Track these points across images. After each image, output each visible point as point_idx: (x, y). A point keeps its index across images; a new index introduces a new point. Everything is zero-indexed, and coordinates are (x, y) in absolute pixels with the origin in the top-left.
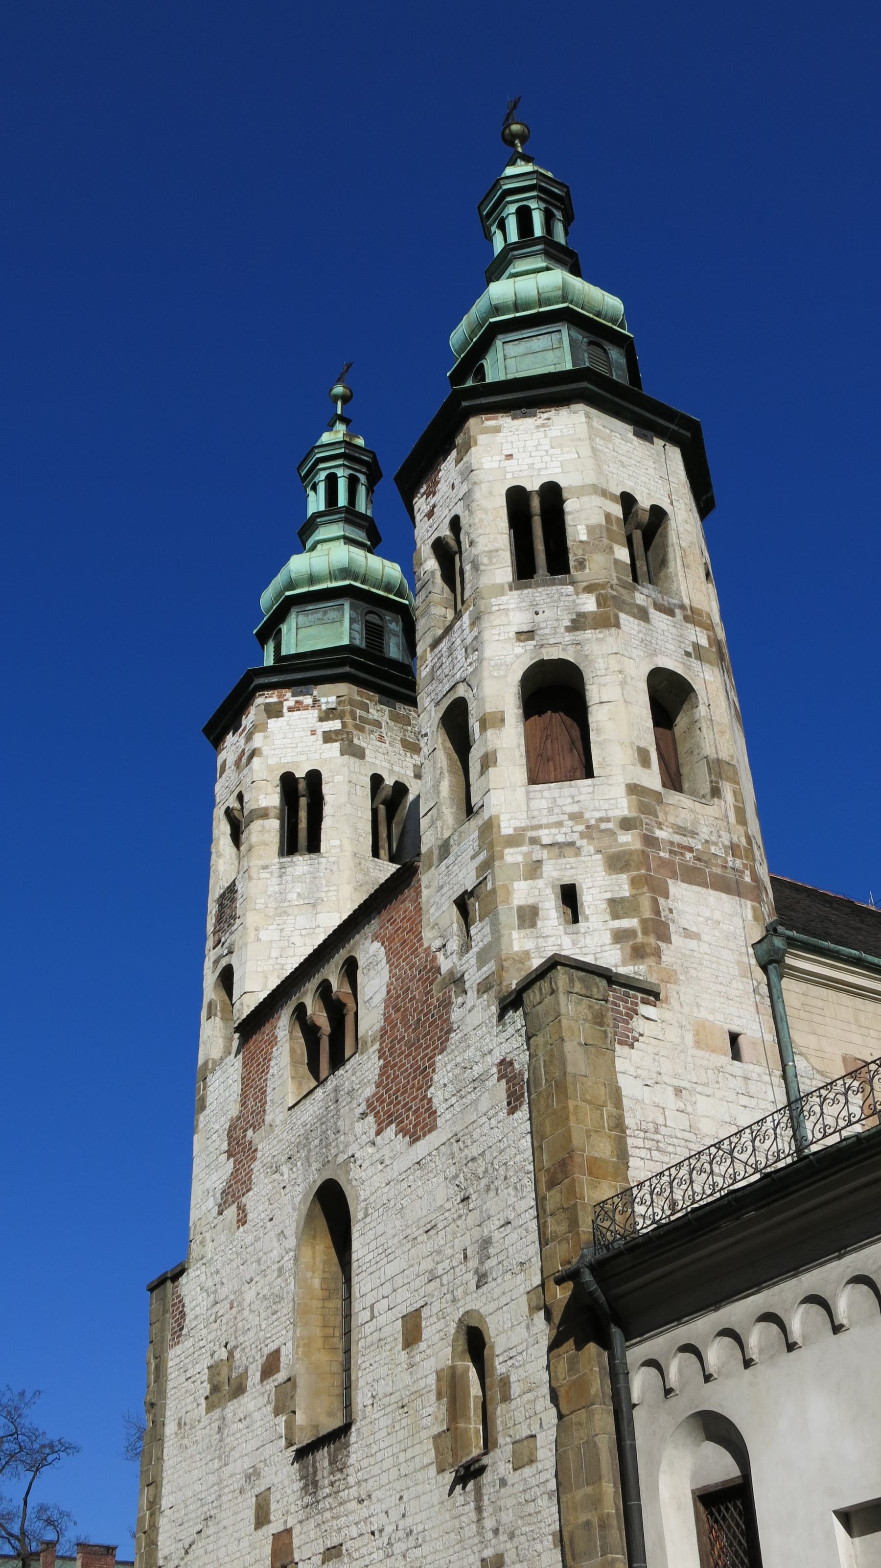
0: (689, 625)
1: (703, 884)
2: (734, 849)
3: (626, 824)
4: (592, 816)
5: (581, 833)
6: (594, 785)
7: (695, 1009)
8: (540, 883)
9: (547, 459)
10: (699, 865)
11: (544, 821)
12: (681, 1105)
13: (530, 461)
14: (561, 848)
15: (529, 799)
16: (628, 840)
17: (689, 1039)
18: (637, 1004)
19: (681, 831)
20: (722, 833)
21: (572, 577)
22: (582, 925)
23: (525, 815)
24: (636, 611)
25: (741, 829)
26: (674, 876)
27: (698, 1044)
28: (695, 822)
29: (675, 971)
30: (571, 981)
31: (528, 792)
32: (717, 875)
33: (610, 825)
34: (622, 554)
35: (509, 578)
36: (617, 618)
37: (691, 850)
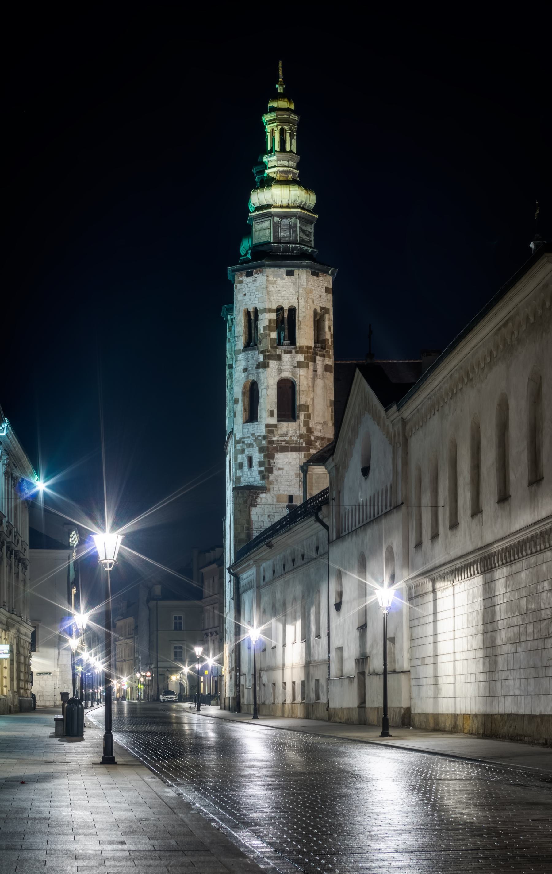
0: (298, 355)
1: (288, 451)
2: (301, 436)
3: (264, 437)
4: (257, 434)
5: (254, 440)
6: (258, 424)
7: (278, 491)
8: (244, 456)
9: (254, 296)
10: (287, 445)
11: (246, 436)
12: (269, 520)
13: (250, 297)
14: (250, 445)
15: (243, 428)
16: (264, 442)
17: (275, 500)
18: (259, 494)
19: (282, 436)
20: (298, 432)
21: (258, 347)
22: (252, 468)
23: (241, 434)
24: (276, 357)
25: (305, 428)
26: (277, 451)
27: (278, 501)
28: (287, 432)
29: (273, 482)
30: (238, 494)
31: (243, 426)
32: (293, 447)
33: (260, 438)
34: (274, 335)
35: (242, 348)
36: (268, 363)
37: (284, 441)
